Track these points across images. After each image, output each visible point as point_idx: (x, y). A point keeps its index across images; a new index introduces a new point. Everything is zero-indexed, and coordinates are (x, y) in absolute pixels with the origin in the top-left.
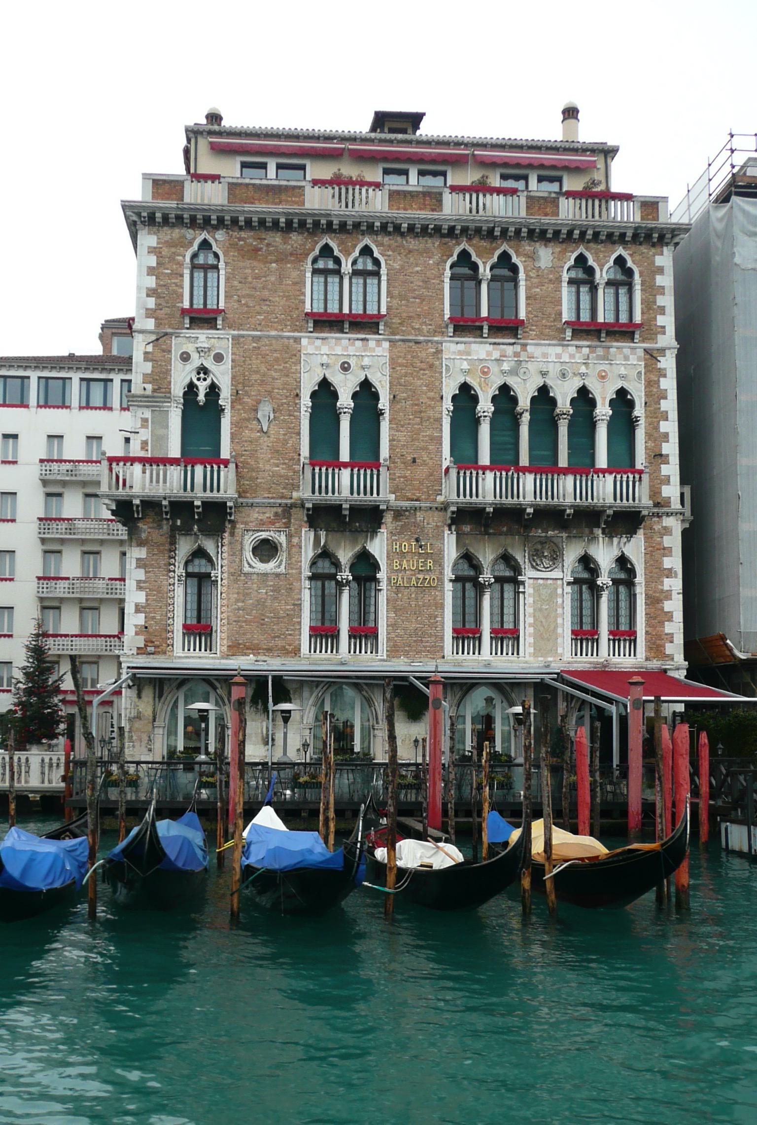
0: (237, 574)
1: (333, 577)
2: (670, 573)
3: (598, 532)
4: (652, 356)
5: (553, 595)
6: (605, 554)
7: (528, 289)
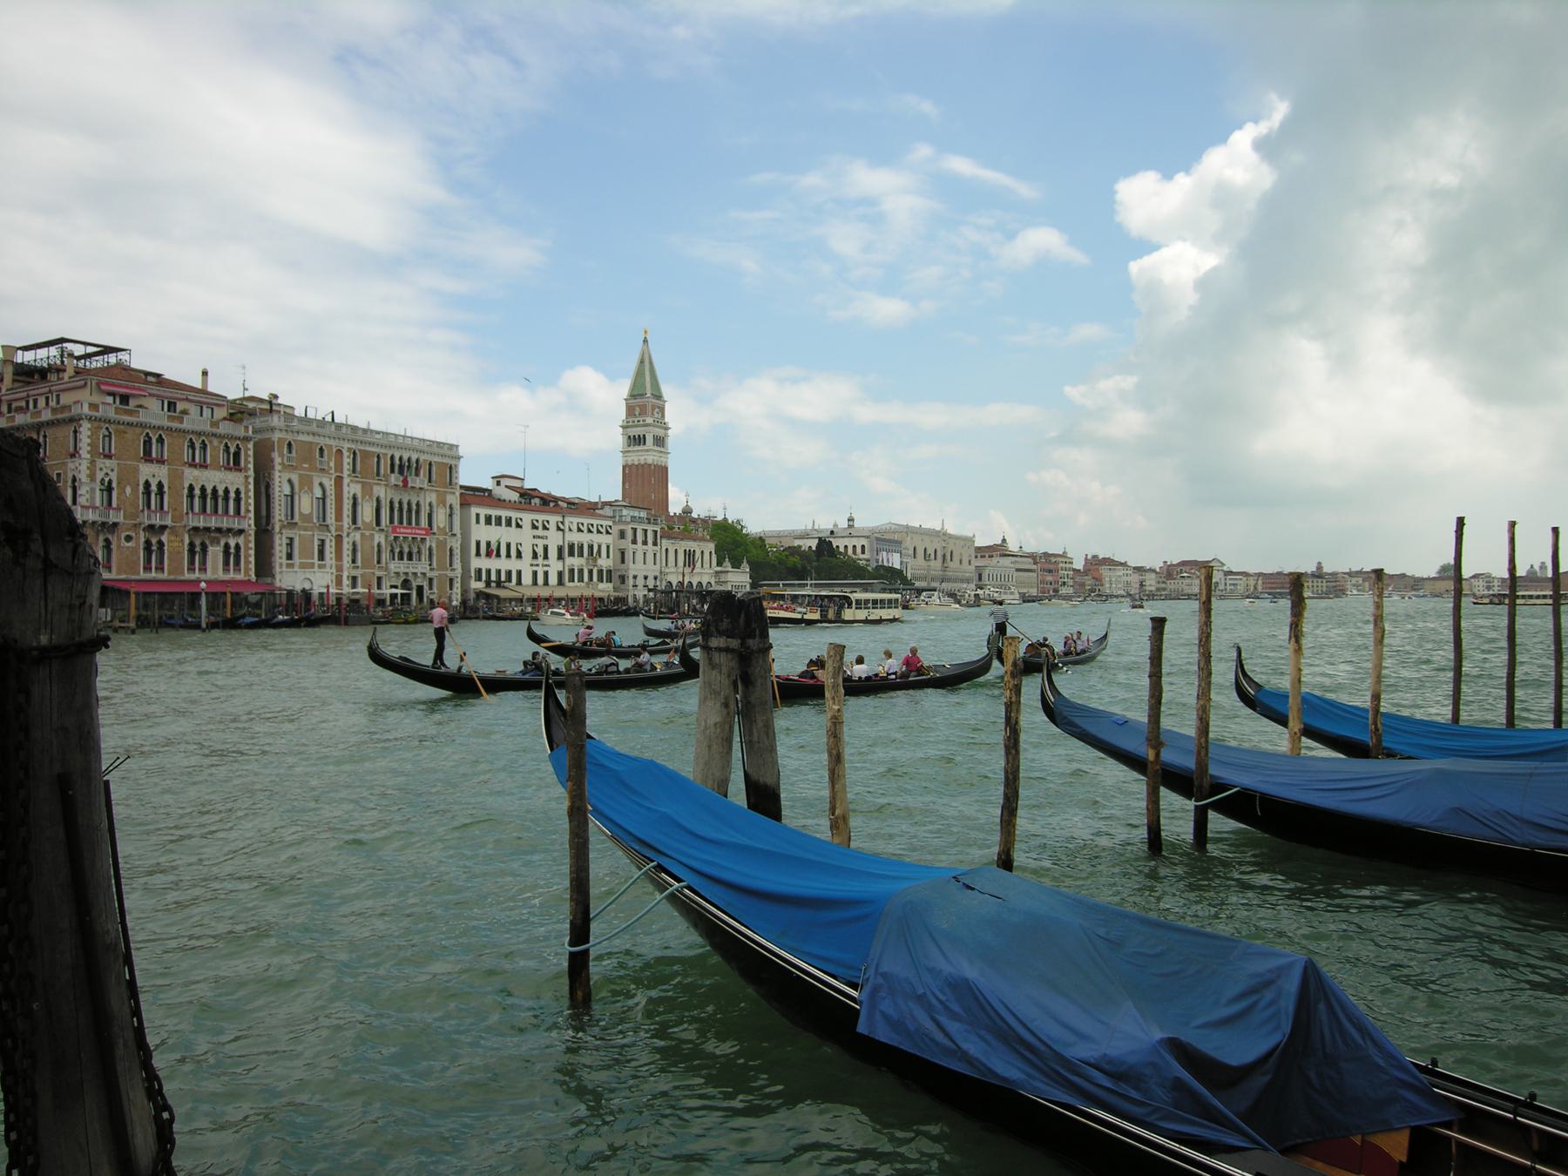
0: (119, 546)
4: (247, 477)
6: (232, 543)
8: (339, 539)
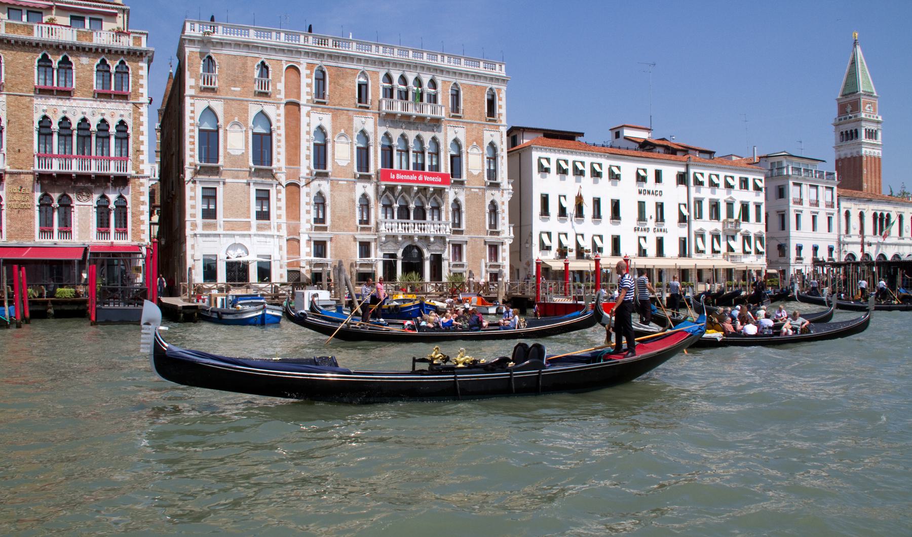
1: (50, 205)
2: (143, 203)
3: (109, 184)
5: (88, 213)
7: (77, 73)
8: (293, 187)
